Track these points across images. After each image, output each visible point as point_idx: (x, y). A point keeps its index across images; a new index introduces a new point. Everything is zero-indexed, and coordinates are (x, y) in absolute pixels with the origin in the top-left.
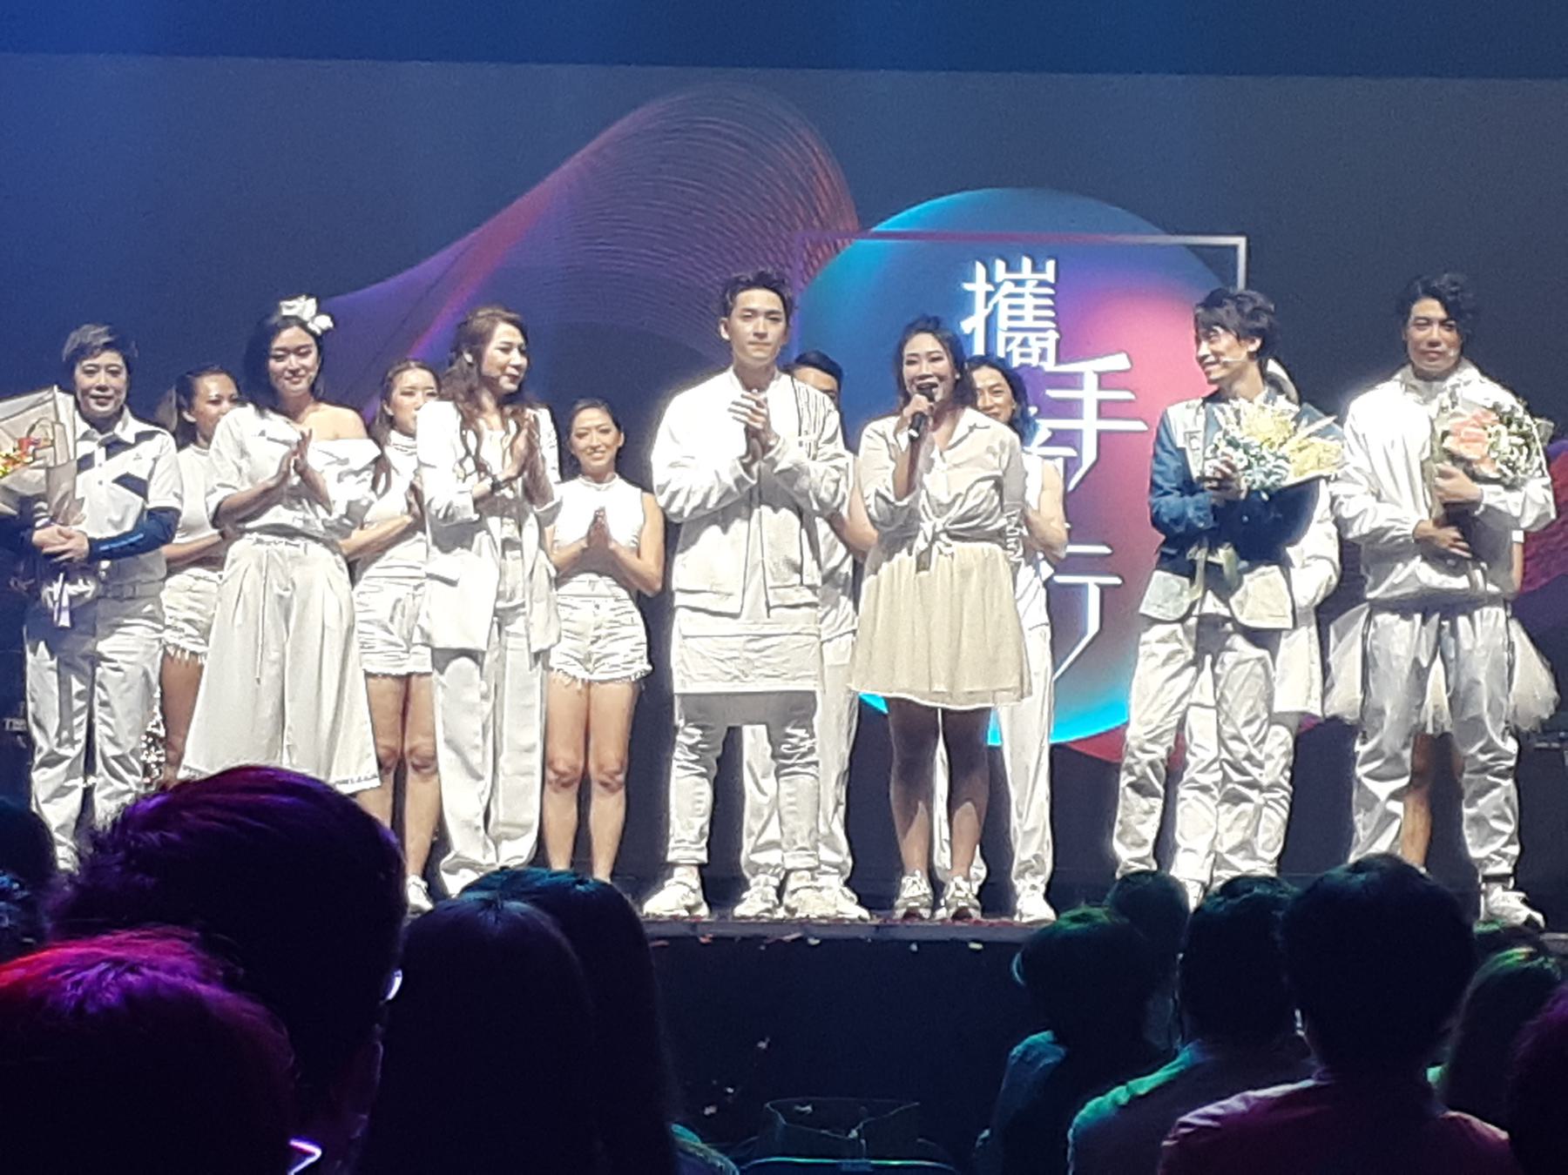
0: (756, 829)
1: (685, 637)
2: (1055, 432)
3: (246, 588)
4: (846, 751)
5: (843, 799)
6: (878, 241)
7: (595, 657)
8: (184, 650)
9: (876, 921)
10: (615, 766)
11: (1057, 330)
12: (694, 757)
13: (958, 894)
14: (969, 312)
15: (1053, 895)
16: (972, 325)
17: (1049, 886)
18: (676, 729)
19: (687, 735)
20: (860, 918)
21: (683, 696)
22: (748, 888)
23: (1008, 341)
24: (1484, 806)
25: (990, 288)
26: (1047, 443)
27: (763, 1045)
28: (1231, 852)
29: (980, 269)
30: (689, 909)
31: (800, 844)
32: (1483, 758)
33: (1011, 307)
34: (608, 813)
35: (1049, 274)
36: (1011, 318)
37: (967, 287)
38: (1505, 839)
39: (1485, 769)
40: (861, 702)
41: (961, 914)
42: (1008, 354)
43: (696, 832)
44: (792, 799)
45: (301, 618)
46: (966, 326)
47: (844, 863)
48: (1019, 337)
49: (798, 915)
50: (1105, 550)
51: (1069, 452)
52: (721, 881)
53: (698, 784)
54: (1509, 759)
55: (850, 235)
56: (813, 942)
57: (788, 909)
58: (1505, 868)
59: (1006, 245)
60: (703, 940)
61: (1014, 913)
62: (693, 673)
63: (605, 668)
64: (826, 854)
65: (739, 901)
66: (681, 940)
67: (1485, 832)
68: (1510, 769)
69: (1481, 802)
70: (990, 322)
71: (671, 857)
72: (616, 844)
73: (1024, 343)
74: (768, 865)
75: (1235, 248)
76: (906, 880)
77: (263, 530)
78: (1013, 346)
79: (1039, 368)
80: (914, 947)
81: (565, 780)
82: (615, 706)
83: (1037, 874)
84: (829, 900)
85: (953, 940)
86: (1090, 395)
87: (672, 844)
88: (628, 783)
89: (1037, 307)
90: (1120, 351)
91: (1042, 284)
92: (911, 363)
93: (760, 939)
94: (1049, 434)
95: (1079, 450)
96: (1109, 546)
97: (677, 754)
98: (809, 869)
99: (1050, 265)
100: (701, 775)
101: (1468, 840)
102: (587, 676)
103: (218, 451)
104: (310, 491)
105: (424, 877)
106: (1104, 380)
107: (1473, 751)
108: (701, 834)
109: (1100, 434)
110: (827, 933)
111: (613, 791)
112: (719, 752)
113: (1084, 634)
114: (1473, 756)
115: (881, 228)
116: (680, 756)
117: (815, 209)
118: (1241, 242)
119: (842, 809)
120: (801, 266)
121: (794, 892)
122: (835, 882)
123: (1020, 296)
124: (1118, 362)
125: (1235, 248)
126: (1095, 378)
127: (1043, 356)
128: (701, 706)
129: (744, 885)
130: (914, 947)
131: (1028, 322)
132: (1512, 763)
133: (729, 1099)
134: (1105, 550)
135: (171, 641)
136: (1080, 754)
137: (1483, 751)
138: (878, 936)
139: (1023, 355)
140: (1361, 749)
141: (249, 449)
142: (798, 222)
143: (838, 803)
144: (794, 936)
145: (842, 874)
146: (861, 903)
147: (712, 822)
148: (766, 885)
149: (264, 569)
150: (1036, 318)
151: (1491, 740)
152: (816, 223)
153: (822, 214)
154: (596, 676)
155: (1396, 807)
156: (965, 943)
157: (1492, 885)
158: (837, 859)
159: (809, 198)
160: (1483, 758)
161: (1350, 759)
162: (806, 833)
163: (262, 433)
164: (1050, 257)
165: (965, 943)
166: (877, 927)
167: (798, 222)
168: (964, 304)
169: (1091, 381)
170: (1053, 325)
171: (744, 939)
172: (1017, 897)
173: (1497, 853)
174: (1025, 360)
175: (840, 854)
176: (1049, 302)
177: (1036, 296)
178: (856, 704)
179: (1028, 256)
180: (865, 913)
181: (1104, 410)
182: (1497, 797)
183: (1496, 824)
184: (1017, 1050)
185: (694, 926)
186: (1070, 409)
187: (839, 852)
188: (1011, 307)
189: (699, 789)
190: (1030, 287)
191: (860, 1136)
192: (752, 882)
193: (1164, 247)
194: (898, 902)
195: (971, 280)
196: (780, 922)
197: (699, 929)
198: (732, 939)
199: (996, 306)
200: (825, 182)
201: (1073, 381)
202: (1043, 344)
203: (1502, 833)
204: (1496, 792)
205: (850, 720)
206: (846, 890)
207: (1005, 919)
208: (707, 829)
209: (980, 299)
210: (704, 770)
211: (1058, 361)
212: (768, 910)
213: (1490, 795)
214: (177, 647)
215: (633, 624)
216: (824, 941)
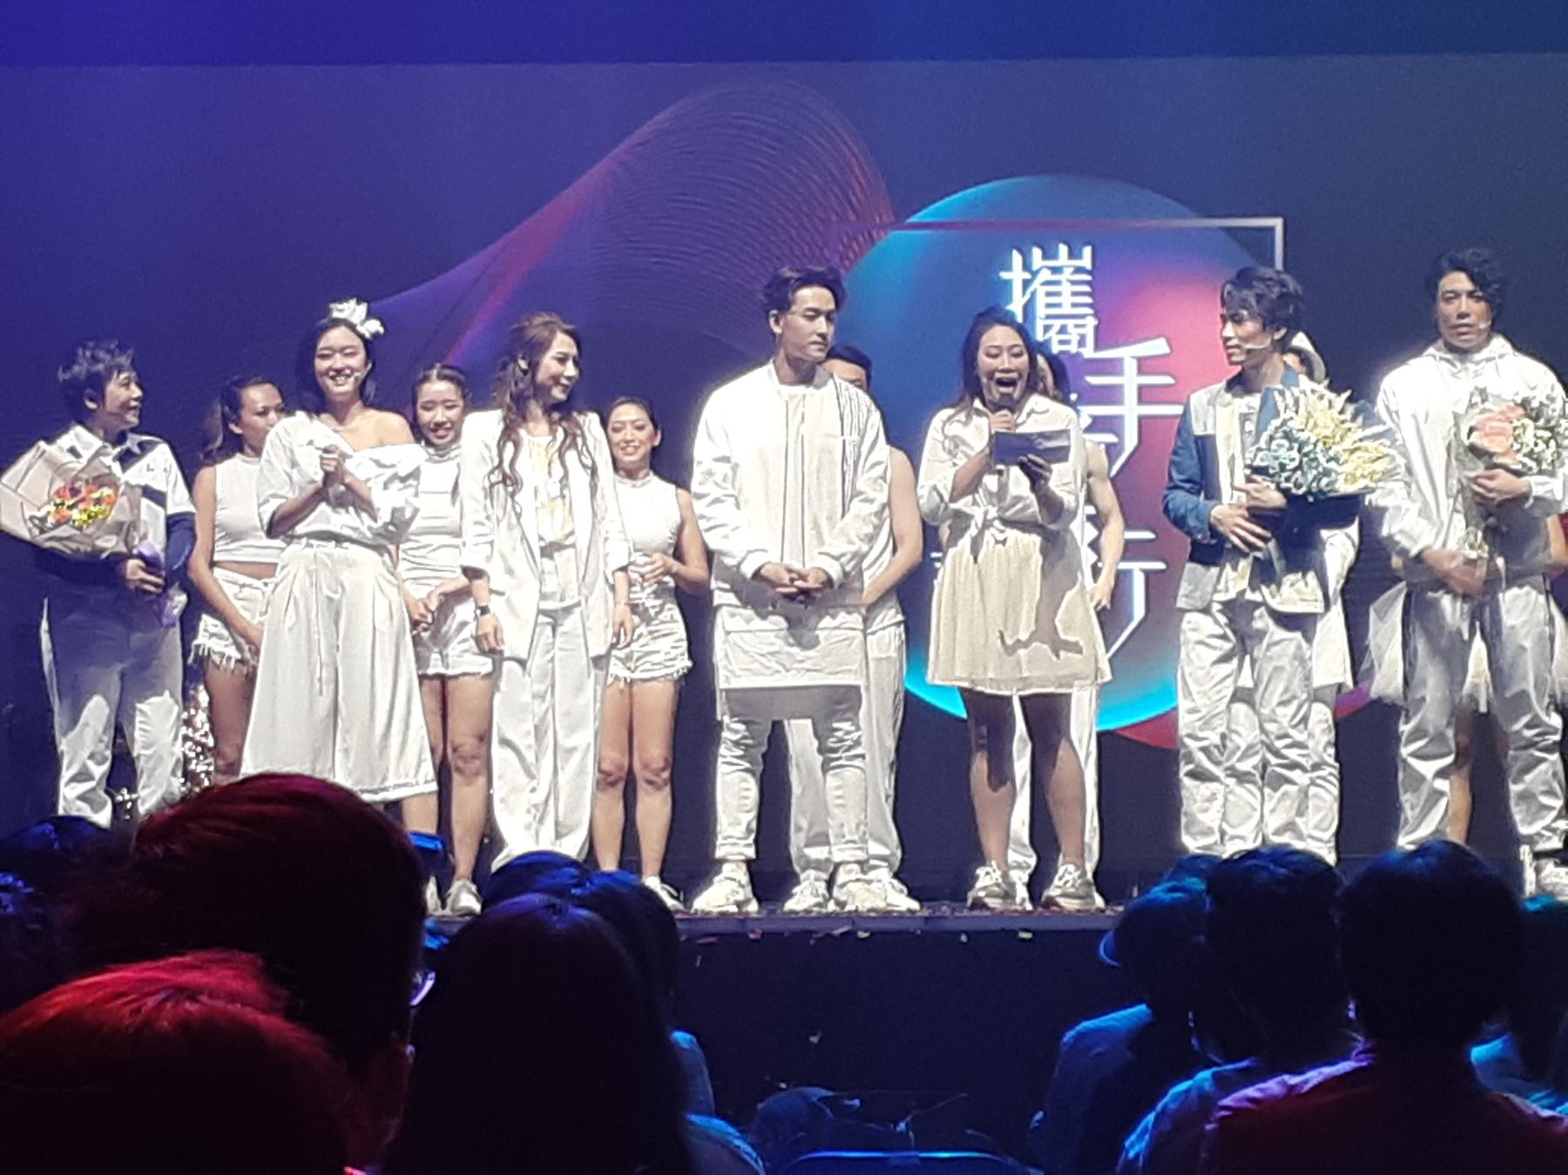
0: (804, 824)
1: (728, 633)
2: (1095, 419)
5: (891, 792)
7: (636, 655)
8: (229, 658)
9: (926, 913)
10: (661, 764)
11: (1096, 315)
12: (740, 753)
15: (1104, 879)
18: (720, 724)
19: (732, 730)
20: (909, 910)
21: (727, 691)
22: (798, 883)
23: (1047, 328)
24: (1532, 782)
25: (1027, 276)
26: (1089, 430)
27: (814, 1039)
28: (1277, 832)
29: (1017, 258)
30: (739, 904)
31: (848, 837)
32: (1528, 733)
33: (1049, 294)
34: (654, 811)
35: (1086, 261)
36: (1049, 305)
37: (1004, 275)
38: (1554, 814)
39: (1531, 744)
40: (908, 694)
43: (743, 828)
44: (840, 793)
47: (893, 854)
48: (1057, 324)
49: (848, 908)
50: (1149, 535)
51: (1111, 438)
52: (771, 873)
53: (745, 780)
54: (1555, 733)
55: (884, 227)
56: (863, 935)
57: (838, 903)
58: (1556, 843)
60: (752, 936)
62: (735, 667)
63: (648, 666)
64: (875, 848)
65: (790, 896)
66: (727, 936)
67: (1534, 809)
68: (1555, 743)
69: (1528, 778)
71: (719, 853)
73: (1063, 330)
74: (818, 861)
75: (1271, 230)
78: (1052, 334)
79: (1078, 355)
80: (964, 938)
81: (610, 779)
82: (658, 702)
84: (879, 893)
86: (1130, 380)
87: (719, 841)
88: (672, 780)
89: (1075, 294)
90: (1158, 336)
91: (1079, 270)
93: (810, 933)
94: (1089, 421)
95: (1119, 433)
96: (1153, 531)
97: (722, 750)
98: (858, 862)
99: (1087, 251)
100: (746, 770)
101: (1517, 818)
102: (628, 674)
104: (354, 499)
105: (474, 881)
106: (1144, 365)
107: (1517, 726)
108: (749, 830)
109: (1142, 420)
111: (659, 788)
112: (764, 749)
113: (1130, 619)
114: (1518, 732)
115: (914, 219)
116: (726, 753)
117: (850, 203)
118: (1277, 223)
119: (891, 800)
121: (843, 885)
122: (884, 874)
123: (1058, 283)
124: (1158, 347)
125: (1271, 230)
126: (1134, 363)
127: (1082, 343)
128: (744, 702)
129: (793, 879)
130: (964, 938)
132: (1557, 738)
134: (1149, 535)
135: (217, 649)
136: (1125, 738)
137: (1528, 726)
138: (927, 928)
139: (1062, 342)
140: (1405, 728)
142: (834, 217)
143: (887, 797)
145: (890, 866)
146: (912, 894)
147: (759, 817)
148: (817, 879)
150: (1074, 305)
151: (1537, 716)
152: (853, 218)
154: (637, 675)
155: (1442, 785)
156: (1015, 933)
157: (1543, 862)
158: (885, 851)
160: (1528, 733)
161: (1396, 739)
162: (853, 826)
164: (1087, 244)
165: (1015, 933)
166: (927, 919)
169: (1130, 367)
170: (1090, 311)
173: (1547, 828)
174: (1064, 348)
175: (887, 845)
176: (1087, 289)
177: (1074, 283)
178: (901, 696)
179: (1065, 243)
180: (915, 905)
181: (1145, 394)
182: (1546, 772)
183: (1545, 800)
184: (1070, 1035)
186: (1110, 395)
187: (886, 845)
188: (1049, 294)
189: (744, 785)
190: (1067, 274)
192: (802, 877)
193: (1199, 230)
196: (828, 916)
197: (750, 925)
198: (782, 934)
201: (1112, 367)
202: (1081, 331)
203: (1550, 808)
204: (1543, 767)
205: (896, 709)
206: (895, 882)
208: (754, 825)
209: (1017, 288)
210: (747, 765)
211: (1097, 347)
212: (818, 905)
213: (1536, 771)
214: (222, 655)
215: (672, 620)
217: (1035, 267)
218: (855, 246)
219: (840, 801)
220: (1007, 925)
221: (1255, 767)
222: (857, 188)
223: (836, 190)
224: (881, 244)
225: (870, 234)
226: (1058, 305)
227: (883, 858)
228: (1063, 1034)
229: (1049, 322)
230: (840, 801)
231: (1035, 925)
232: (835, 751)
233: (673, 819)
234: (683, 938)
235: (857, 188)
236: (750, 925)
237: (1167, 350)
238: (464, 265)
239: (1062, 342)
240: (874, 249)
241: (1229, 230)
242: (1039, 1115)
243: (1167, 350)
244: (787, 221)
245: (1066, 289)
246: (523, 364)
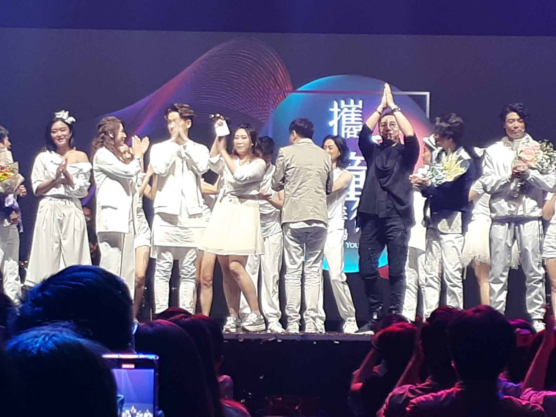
3: (47, 217)
9: (302, 334)
16: (333, 123)
23: (346, 129)
25: (340, 110)
27: (261, 378)
29: (336, 104)
33: (347, 117)
35: (360, 105)
36: (347, 121)
37: (331, 110)
42: (346, 134)
44: (186, 290)
45: (67, 228)
46: (331, 124)
48: (349, 127)
59: (345, 95)
60: (240, 341)
70: (339, 122)
72: (210, 306)
73: (351, 130)
75: (425, 96)
77: (51, 196)
78: (348, 131)
80: (315, 343)
89: (356, 117)
91: (358, 109)
93: (260, 340)
97: (157, 273)
99: (361, 102)
103: (37, 168)
117: (277, 82)
118: (428, 94)
120: (272, 102)
125: (425, 96)
130: (315, 343)
131: (353, 122)
133: (250, 397)
138: (302, 339)
139: (351, 134)
141: (47, 168)
142: (271, 88)
144: (272, 339)
145: (278, 317)
149: (53, 211)
150: (356, 121)
152: (278, 88)
159: (275, 78)
163: (52, 162)
165: (333, 342)
166: (302, 336)
167: (271, 88)
168: (330, 116)
174: (352, 136)
176: (360, 115)
179: (353, 99)
185: (237, 335)
188: (347, 117)
190: (353, 110)
191: (299, 409)
195: (333, 107)
197: (240, 336)
199: (341, 116)
209: (336, 114)
216: (283, 341)
217: (342, 107)
218: (279, 99)
219: (186, 293)
222: (280, 78)
223: (273, 78)
224: (287, 98)
225: (284, 93)
227: (275, 314)
230: (186, 293)
232: (186, 275)
235: (280, 78)
236: (240, 336)
238: (141, 101)
239: (351, 134)
240: (285, 100)
241: (409, 96)
245: (353, 115)
246: (111, 136)
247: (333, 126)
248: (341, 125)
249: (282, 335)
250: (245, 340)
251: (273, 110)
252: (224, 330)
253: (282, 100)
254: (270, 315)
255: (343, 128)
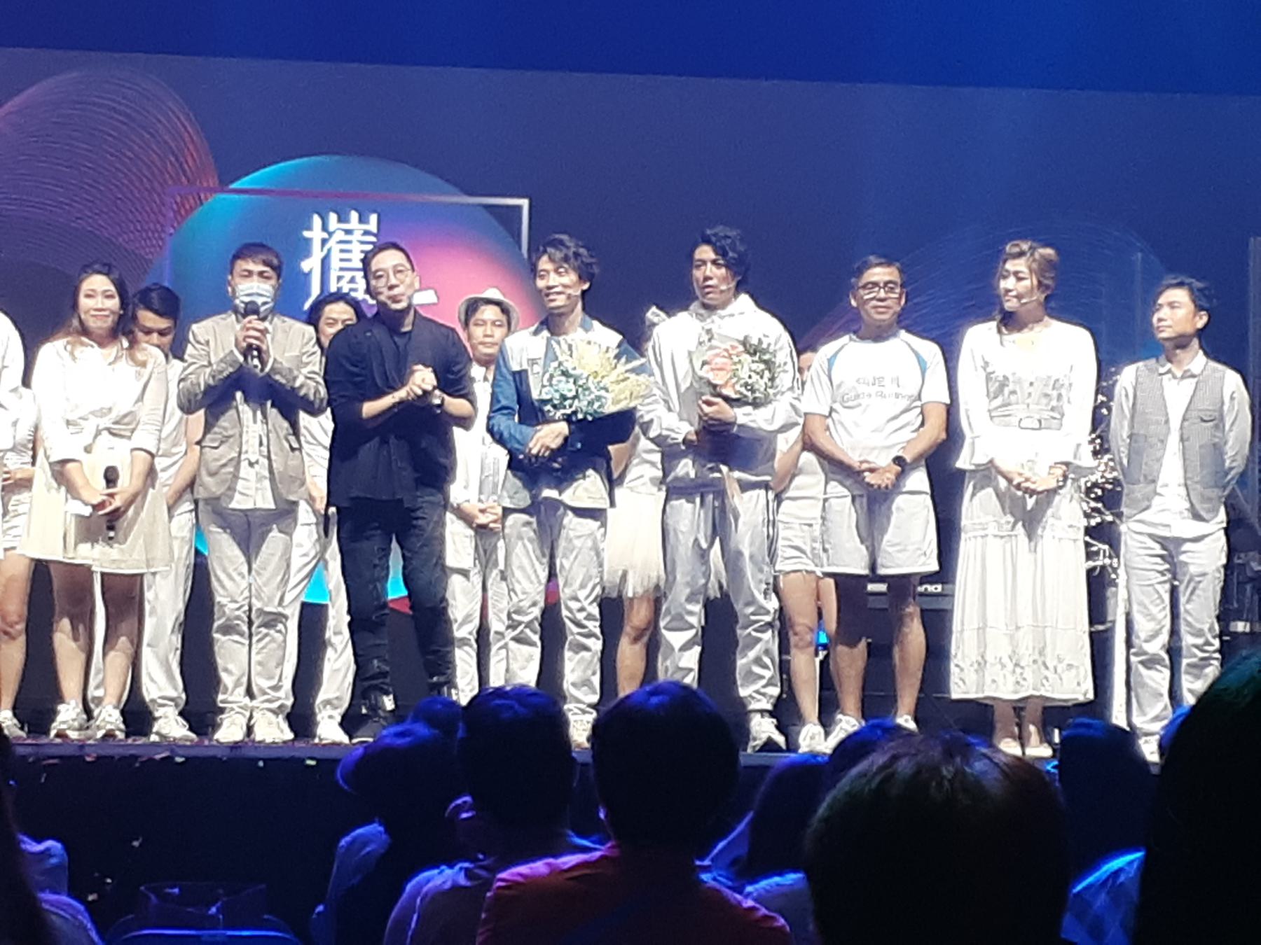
4: (181, 606)
6: (236, 196)
10: (14, 618)
13: (108, 719)
14: (307, 253)
16: (311, 265)
17: (344, 717)
23: (339, 278)
25: (325, 235)
27: (136, 844)
29: (317, 220)
33: (342, 251)
35: (373, 225)
36: (342, 260)
37: (306, 234)
41: (109, 735)
46: (306, 266)
55: (213, 191)
56: (179, 760)
59: (340, 202)
60: (88, 759)
61: (314, 736)
70: (325, 262)
73: (352, 280)
75: (519, 208)
76: (61, 707)
83: (336, 708)
85: (292, 758)
90: (429, 288)
91: (366, 233)
92: (88, 296)
93: (135, 757)
99: (374, 218)
110: (193, 753)
111: (13, 638)
115: (234, 186)
118: (524, 203)
120: (171, 214)
125: (519, 208)
130: (261, 764)
133: (108, 888)
142: (170, 182)
144: (163, 755)
145: (177, 706)
152: (183, 179)
153: (189, 173)
164: (374, 211)
165: (304, 760)
167: (170, 182)
168: (304, 248)
171: (123, 758)
172: (315, 724)
177: (363, 243)
179: (356, 210)
188: (342, 251)
190: (357, 236)
194: (54, 725)
195: (310, 228)
196: (154, 743)
197: (87, 750)
198: (112, 757)
199: (329, 250)
200: (191, 147)
207: (141, 741)
209: (316, 245)
216: (187, 759)
217: (331, 229)
218: (188, 207)
220: (297, 754)
221: (470, 633)
223: (173, 159)
226: (349, 260)
227: (172, 699)
228: (339, 841)
229: (341, 273)
231: (318, 756)
233: (25, 665)
234: (31, 760)
236: (87, 750)
237: (434, 300)
242: (320, 908)
243: (434, 300)
244: (131, 182)
247: (310, 272)
248: (329, 269)
249: (185, 746)
250: (99, 758)
251: (172, 231)
252: (53, 733)
253: (192, 209)
254: (160, 701)
255: (333, 275)
